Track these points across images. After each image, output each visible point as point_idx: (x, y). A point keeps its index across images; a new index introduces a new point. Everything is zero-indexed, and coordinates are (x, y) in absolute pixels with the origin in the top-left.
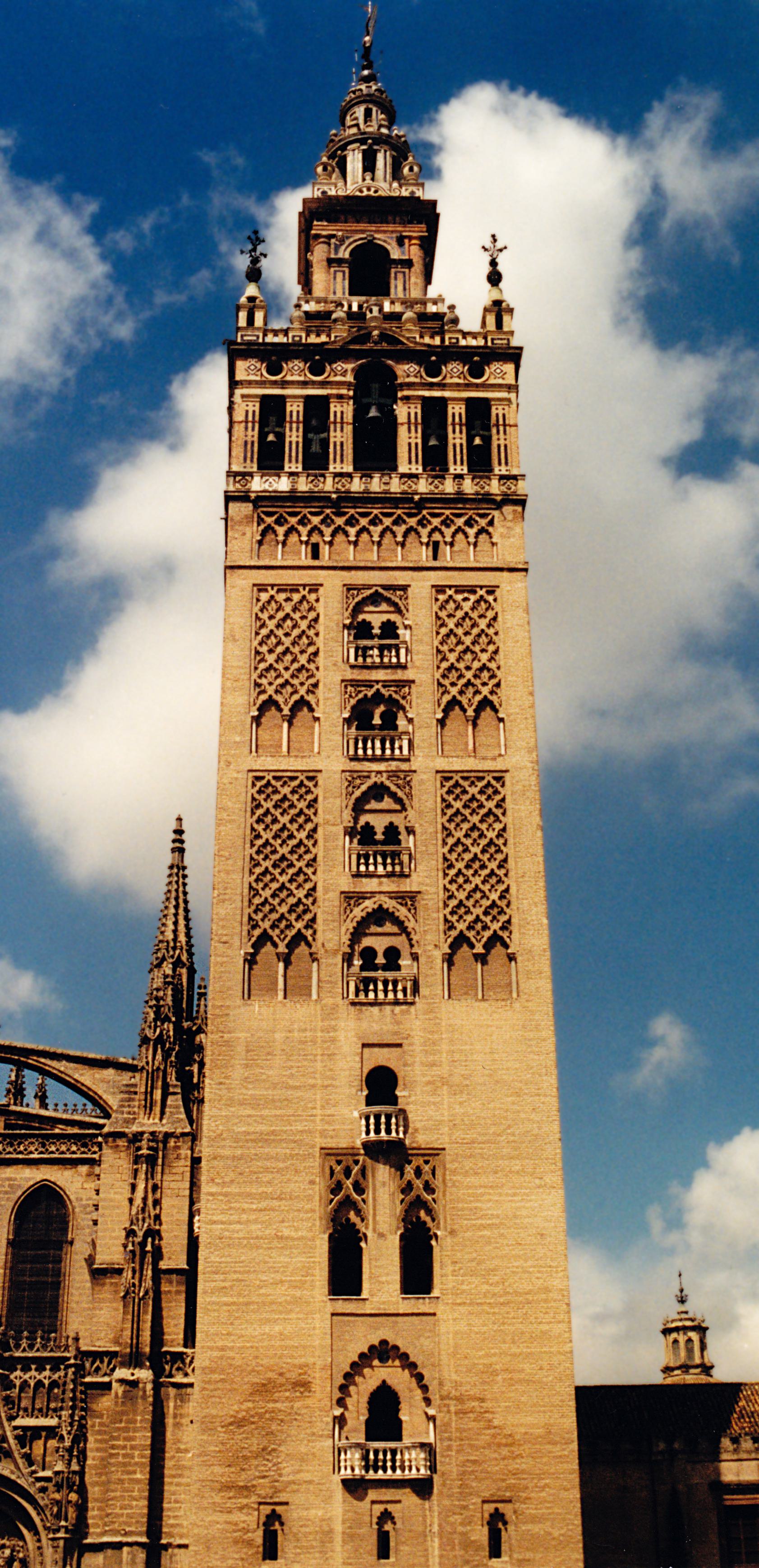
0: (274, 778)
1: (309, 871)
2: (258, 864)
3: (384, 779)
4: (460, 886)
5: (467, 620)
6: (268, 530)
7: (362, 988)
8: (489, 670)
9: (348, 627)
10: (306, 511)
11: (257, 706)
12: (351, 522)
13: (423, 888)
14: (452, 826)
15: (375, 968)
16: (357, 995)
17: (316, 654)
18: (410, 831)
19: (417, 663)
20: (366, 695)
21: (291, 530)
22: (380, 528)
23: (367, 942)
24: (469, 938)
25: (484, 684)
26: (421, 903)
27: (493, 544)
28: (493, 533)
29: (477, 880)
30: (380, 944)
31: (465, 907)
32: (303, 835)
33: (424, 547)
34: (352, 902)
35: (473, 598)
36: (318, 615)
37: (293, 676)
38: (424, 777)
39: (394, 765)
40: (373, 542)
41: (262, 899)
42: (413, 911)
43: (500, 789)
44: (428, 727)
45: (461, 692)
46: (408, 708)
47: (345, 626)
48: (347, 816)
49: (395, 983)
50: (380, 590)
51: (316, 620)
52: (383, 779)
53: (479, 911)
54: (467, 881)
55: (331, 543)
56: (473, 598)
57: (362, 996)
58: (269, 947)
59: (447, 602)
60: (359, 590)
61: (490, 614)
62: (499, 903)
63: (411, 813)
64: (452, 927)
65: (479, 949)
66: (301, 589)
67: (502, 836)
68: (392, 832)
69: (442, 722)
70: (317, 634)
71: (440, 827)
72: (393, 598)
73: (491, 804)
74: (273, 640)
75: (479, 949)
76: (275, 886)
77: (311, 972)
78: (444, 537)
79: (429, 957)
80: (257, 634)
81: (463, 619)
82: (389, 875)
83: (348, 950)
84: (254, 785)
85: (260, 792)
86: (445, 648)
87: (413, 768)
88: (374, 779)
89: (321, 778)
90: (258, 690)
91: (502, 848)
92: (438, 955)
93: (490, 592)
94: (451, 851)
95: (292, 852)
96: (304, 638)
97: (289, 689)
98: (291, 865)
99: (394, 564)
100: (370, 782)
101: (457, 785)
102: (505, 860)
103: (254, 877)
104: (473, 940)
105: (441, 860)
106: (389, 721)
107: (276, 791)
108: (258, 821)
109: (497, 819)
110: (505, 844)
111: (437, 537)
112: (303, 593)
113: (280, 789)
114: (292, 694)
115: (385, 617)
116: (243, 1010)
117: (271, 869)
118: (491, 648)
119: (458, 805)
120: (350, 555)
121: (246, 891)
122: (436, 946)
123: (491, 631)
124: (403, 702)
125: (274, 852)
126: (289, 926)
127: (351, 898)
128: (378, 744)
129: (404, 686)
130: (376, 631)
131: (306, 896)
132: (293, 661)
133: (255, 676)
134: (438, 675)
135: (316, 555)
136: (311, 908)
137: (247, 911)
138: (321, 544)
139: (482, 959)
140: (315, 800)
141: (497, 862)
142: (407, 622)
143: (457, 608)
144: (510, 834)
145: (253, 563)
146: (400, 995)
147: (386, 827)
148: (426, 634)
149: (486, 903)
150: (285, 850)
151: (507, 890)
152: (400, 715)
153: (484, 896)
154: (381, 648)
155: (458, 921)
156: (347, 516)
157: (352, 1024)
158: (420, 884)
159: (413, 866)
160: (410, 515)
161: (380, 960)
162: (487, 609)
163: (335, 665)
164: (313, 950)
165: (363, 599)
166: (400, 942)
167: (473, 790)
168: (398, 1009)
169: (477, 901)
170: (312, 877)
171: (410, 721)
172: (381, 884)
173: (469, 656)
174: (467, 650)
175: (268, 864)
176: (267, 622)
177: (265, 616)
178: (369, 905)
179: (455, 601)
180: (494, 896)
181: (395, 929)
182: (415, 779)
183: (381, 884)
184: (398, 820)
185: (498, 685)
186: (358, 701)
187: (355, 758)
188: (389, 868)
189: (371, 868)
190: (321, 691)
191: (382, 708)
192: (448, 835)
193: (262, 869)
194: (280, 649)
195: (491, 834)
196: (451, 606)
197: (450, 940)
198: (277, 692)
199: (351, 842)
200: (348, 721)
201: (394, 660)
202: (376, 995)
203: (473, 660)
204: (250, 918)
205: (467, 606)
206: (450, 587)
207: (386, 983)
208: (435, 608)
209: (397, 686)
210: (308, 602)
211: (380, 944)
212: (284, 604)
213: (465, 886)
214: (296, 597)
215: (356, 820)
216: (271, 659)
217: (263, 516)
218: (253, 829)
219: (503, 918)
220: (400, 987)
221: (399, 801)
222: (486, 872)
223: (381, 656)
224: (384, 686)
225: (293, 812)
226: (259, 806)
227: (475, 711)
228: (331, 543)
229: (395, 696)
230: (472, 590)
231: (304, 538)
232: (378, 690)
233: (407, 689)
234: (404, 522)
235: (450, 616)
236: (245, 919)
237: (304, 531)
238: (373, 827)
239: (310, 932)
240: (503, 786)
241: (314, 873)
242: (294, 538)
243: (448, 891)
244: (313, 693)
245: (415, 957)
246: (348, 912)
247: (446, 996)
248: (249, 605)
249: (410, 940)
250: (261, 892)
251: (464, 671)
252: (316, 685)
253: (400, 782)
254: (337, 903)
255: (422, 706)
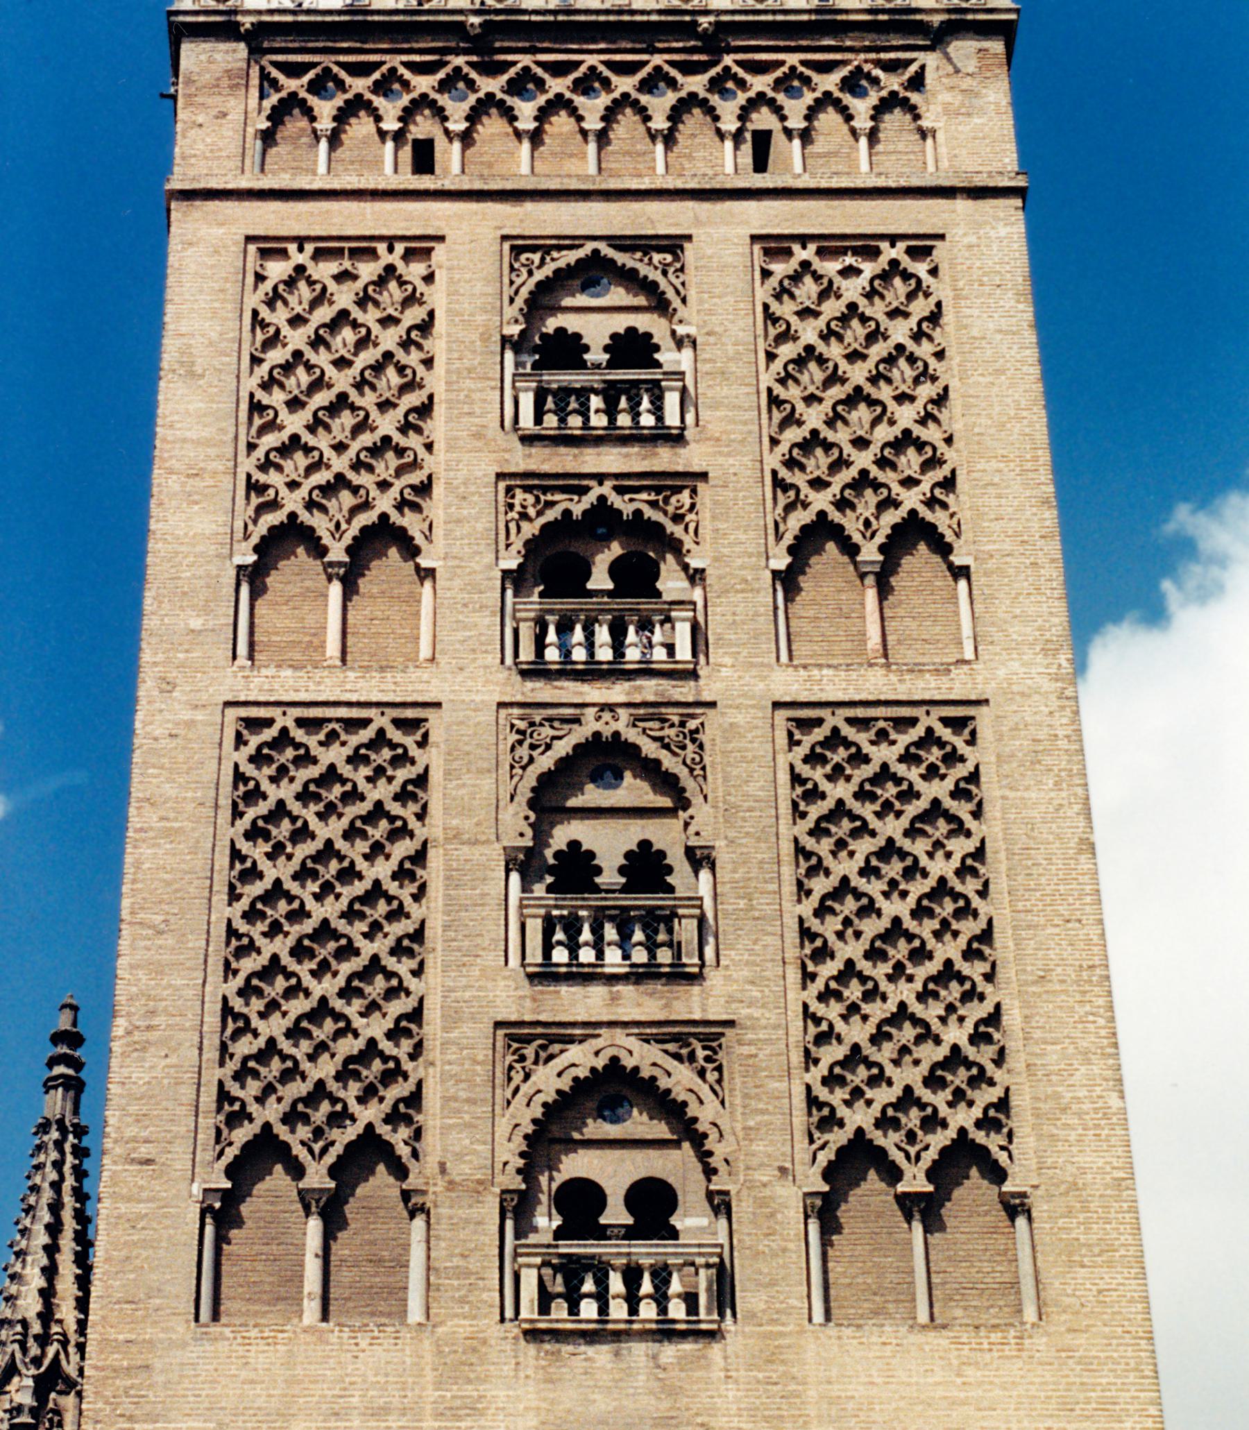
0: (300, 722)
1: (403, 967)
2: (250, 948)
3: (621, 724)
4: (853, 1008)
5: (855, 323)
6: (291, 104)
7: (559, 1286)
8: (920, 445)
9: (517, 345)
10: (395, 61)
11: (255, 540)
12: (522, 85)
13: (740, 1013)
14: (824, 847)
15: (602, 1233)
16: (544, 1309)
17: (425, 410)
18: (699, 859)
19: (714, 428)
20: (567, 513)
21: (356, 106)
22: (603, 100)
23: (576, 1165)
24: (882, 1151)
25: (909, 482)
26: (734, 1051)
27: (923, 134)
28: (922, 110)
29: (905, 992)
30: (615, 1173)
31: (870, 1064)
32: (382, 870)
33: (729, 144)
34: (529, 1051)
35: (869, 269)
36: (431, 314)
37: (357, 465)
38: (740, 718)
39: (649, 689)
40: (584, 133)
41: (261, 1042)
42: (712, 1076)
43: (962, 748)
44: (749, 588)
45: (842, 504)
46: (688, 542)
47: (505, 340)
48: (515, 825)
49: (662, 1275)
50: (606, 250)
51: (425, 327)
52: (621, 726)
53: (910, 1076)
54: (873, 994)
55: (466, 138)
56: (869, 269)
57: (560, 1310)
58: (278, 1179)
59: (796, 278)
60: (547, 250)
61: (920, 308)
62: (970, 1052)
63: (701, 812)
64: (831, 1121)
65: (915, 1181)
66: (382, 248)
67: (974, 872)
68: (646, 867)
69: (788, 581)
70: (428, 363)
71: (787, 848)
72: (644, 270)
73: (939, 789)
74: (303, 377)
75: (915, 1181)
76: (298, 1006)
77: (406, 1247)
78: (783, 118)
79: (762, 1203)
80: (256, 361)
81: (844, 319)
82: (638, 976)
83: (518, 1183)
84: (240, 741)
85: (258, 759)
86: (793, 393)
87: (706, 697)
88: (591, 725)
89: (436, 723)
90: (255, 501)
91: (976, 902)
92: (789, 1201)
93: (919, 253)
94: (822, 911)
95: (350, 915)
96: (391, 372)
97: (347, 499)
98: (349, 951)
99: (645, 184)
100: (579, 734)
101: (835, 739)
102: (986, 936)
103: (239, 981)
104: (897, 1156)
105: (792, 935)
106: (636, 578)
107: (307, 759)
108: (253, 834)
109: (959, 829)
110: (983, 893)
111: (763, 119)
112: (386, 258)
113: (316, 750)
114: (354, 511)
115: (620, 323)
116: (192, 1353)
117: (286, 960)
118: (926, 391)
119: (841, 791)
120: (520, 165)
121: (213, 1020)
122: (783, 1170)
123: (925, 350)
124: (677, 530)
125: (300, 914)
126: (340, 1118)
127: (528, 1040)
128: (603, 634)
129: (678, 490)
130: (596, 355)
131: (391, 1035)
132: (357, 430)
133: (248, 465)
134: (773, 460)
135: (424, 158)
136: (407, 1066)
137: (213, 1074)
138: (440, 143)
139: (926, 1210)
140: (422, 780)
141: (962, 941)
142: (681, 330)
143: (823, 295)
144: (996, 868)
145: (244, 183)
146: (677, 1310)
147: (628, 855)
148: (736, 358)
149: (931, 1054)
150: (330, 909)
151: (994, 1018)
152: (669, 566)
153: (927, 1035)
154: (611, 393)
155: (848, 1103)
156: (512, 72)
157: (530, 1394)
158: (731, 1000)
159: (709, 951)
160: (689, 69)
161: (616, 1214)
162: (911, 296)
163: (478, 436)
164: (412, 1182)
165: (557, 272)
166: (675, 1166)
167: (882, 754)
168: (670, 1352)
169: (904, 1050)
170: (411, 983)
171: (696, 576)
172: (614, 998)
173: (862, 414)
174: (857, 397)
175: (281, 946)
176: (286, 330)
177: (279, 317)
178: (582, 1058)
179: (817, 277)
180: (956, 1035)
181: (660, 1130)
182: (713, 726)
183: (614, 998)
184: (667, 836)
185: (949, 483)
186: (544, 527)
187: (536, 671)
188: (640, 956)
189: (587, 955)
190: (438, 506)
191: (616, 549)
192: (812, 872)
193: (263, 960)
194: (322, 398)
195: (939, 867)
196: (808, 290)
197: (824, 1158)
198: (310, 505)
199: (525, 888)
200: (515, 580)
201: (647, 420)
202: (603, 1309)
203: (875, 422)
204: (223, 1096)
205: (852, 289)
206: (804, 240)
207: (632, 1275)
208: (763, 293)
209: (658, 490)
210: (402, 283)
211: (615, 1173)
212: (332, 286)
213: (866, 1008)
214: (368, 271)
215: (541, 833)
216: (295, 423)
217: (275, 73)
218: (236, 855)
219: (986, 1096)
220: (676, 1286)
221: (666, 782)
222: (933, 967)
223: (611, 411)
224: (620, 490)
225: (354, 810)
226: (255, 795)
227: (882, 549)
228: (466, 138)
229: (649, 513)
230: (867, 247)
231: (390, 125)
232: (602, 499)
233: (686, 493)
234: (673, 84)
235: (806, 313)
236: (209, 1097)
237: (392, 111)
238: (591, 855)
239: (404, 1132)
240: (972, 741)
241: (417, 973)
242: (361, 127)
243: (817, 1021)
244: (416, 508)
245: (720, 1205)
246: (518, 1077)
247: (818, 1316)
248: (233, 289)
249: (704, 1156)
250: (256, 1022)
251: (848, 449)
252: (424, 489)
253: (672, 732)
254: (483, 1053)
255: (731, 537)
